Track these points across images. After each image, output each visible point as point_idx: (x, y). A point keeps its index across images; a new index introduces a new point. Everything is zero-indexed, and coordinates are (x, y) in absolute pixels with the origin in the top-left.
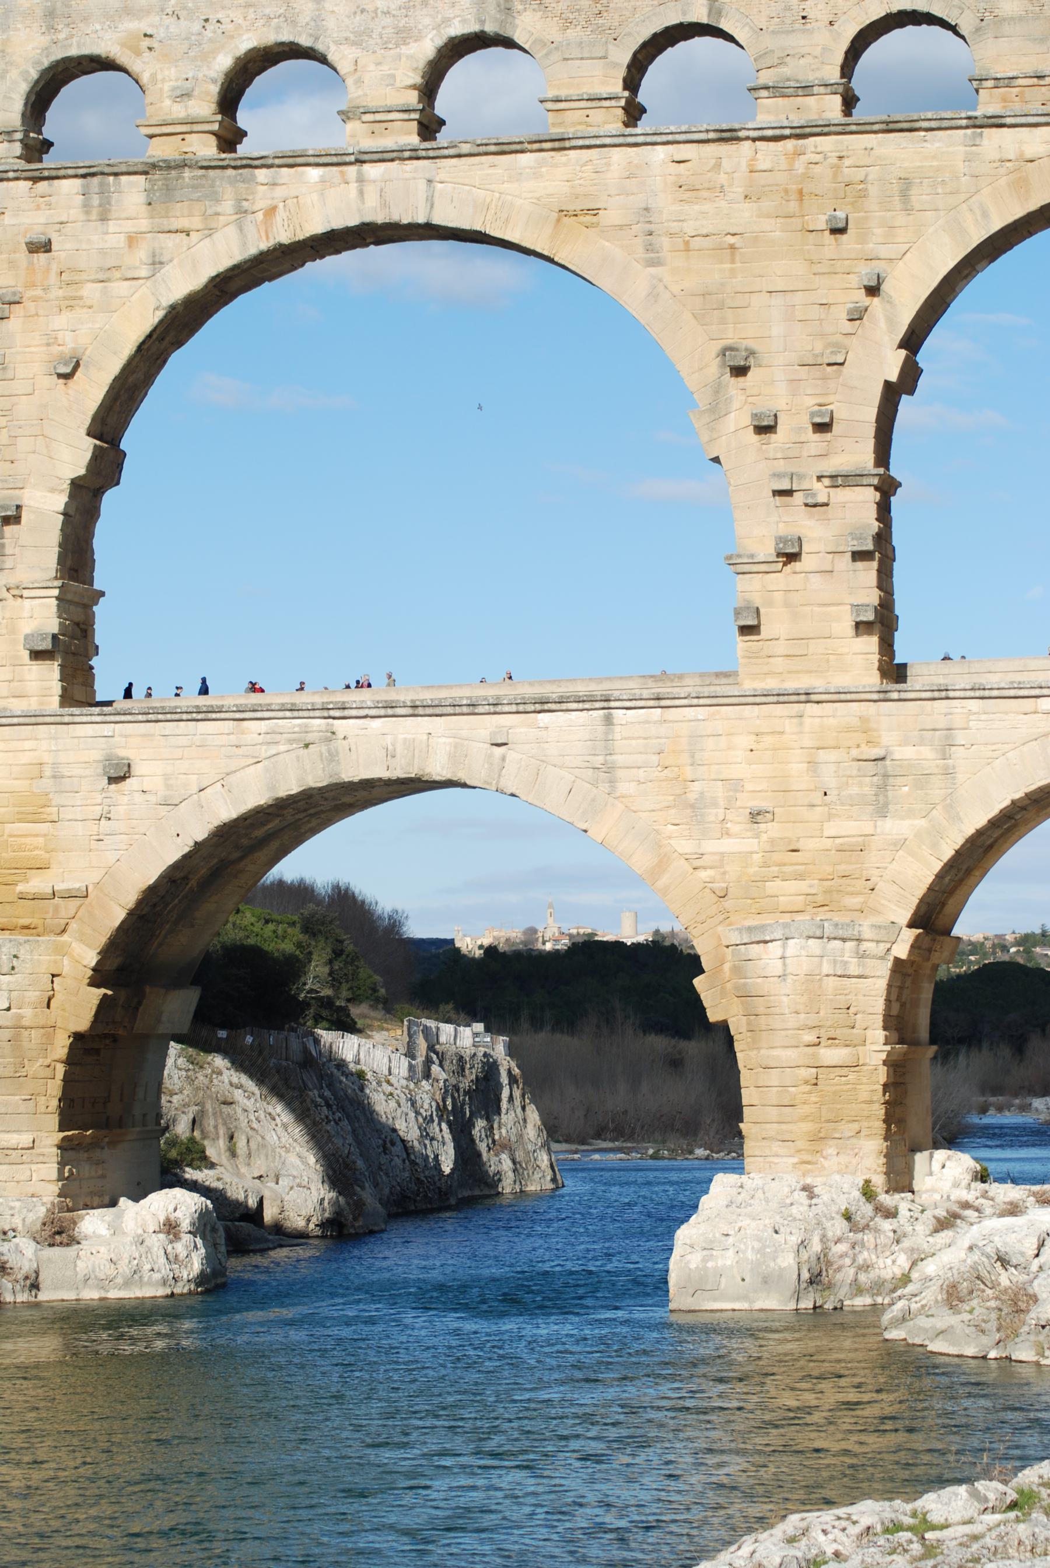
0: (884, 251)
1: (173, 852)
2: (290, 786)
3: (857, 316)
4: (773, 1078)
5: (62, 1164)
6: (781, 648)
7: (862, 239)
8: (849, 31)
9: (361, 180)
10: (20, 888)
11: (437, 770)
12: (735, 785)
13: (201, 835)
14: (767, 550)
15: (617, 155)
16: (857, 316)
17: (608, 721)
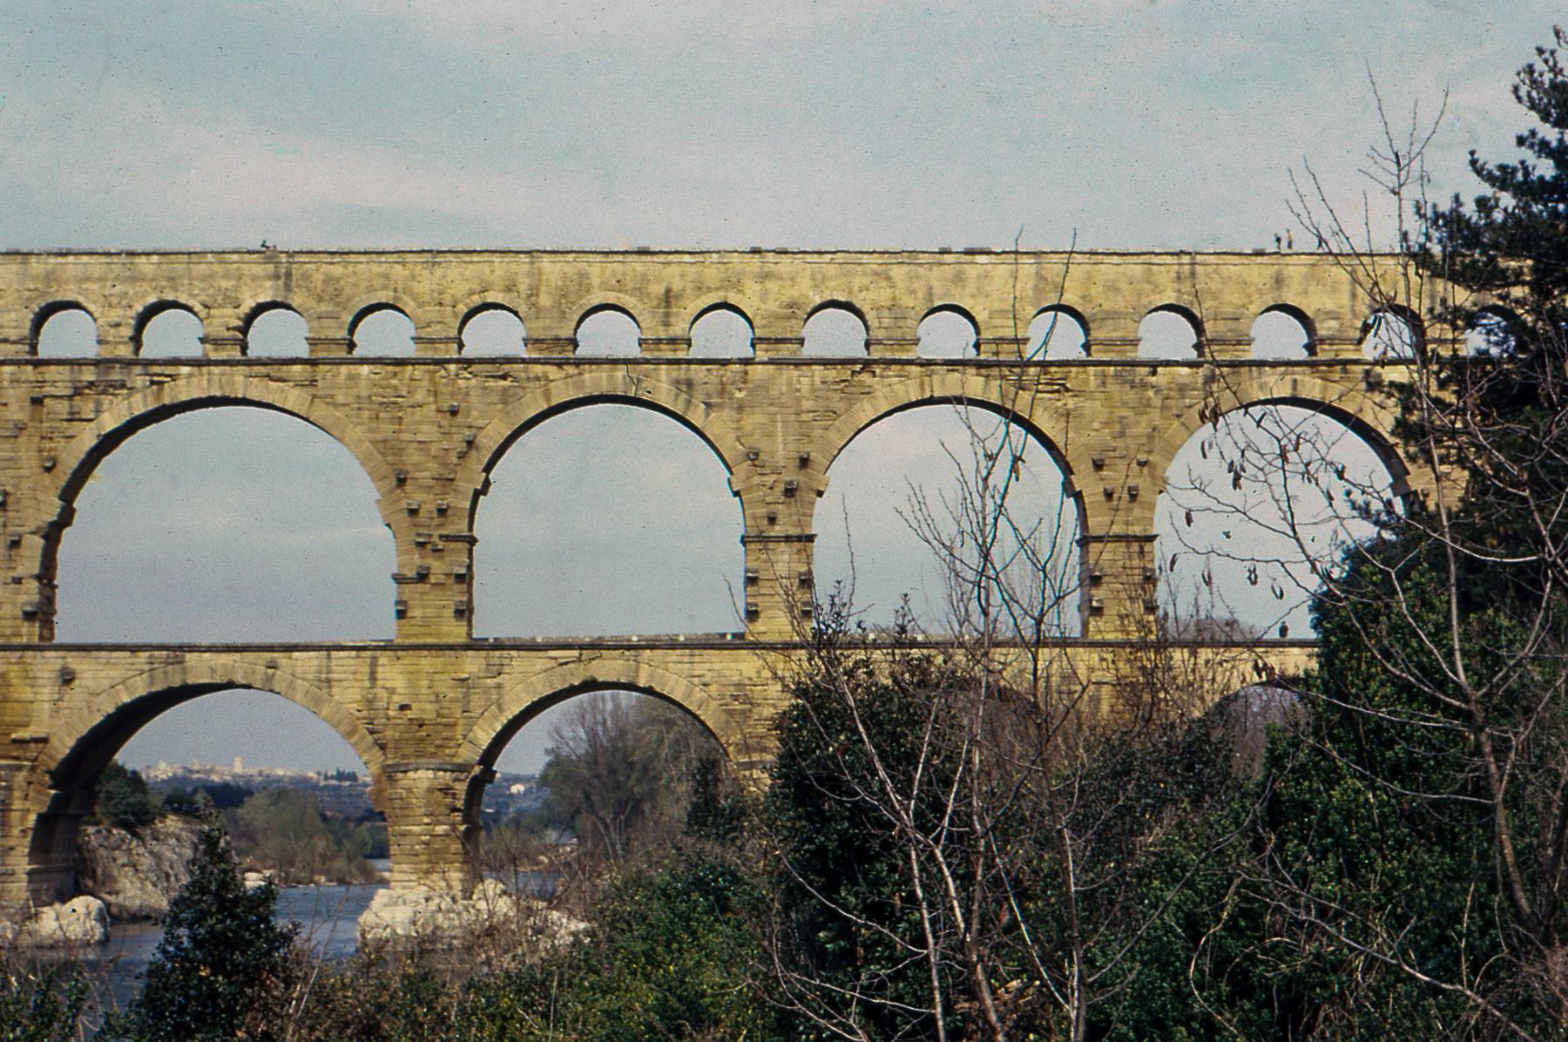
0: (480, 423)
1: (97, 719)
2: (159, 687)
3: (462, 456)
4: (408, 840)
5: (30, 882)
6: (418, 621)
7: (468, 415)
8: (463, 309)
9: (209, 374)
10: (14, 736)
11: (239, 679)
12: (392, 691)
13: (111, 710)
14: (412, 574)
15: (344, 369)
16: (462, 456)
17: (329, 657)
